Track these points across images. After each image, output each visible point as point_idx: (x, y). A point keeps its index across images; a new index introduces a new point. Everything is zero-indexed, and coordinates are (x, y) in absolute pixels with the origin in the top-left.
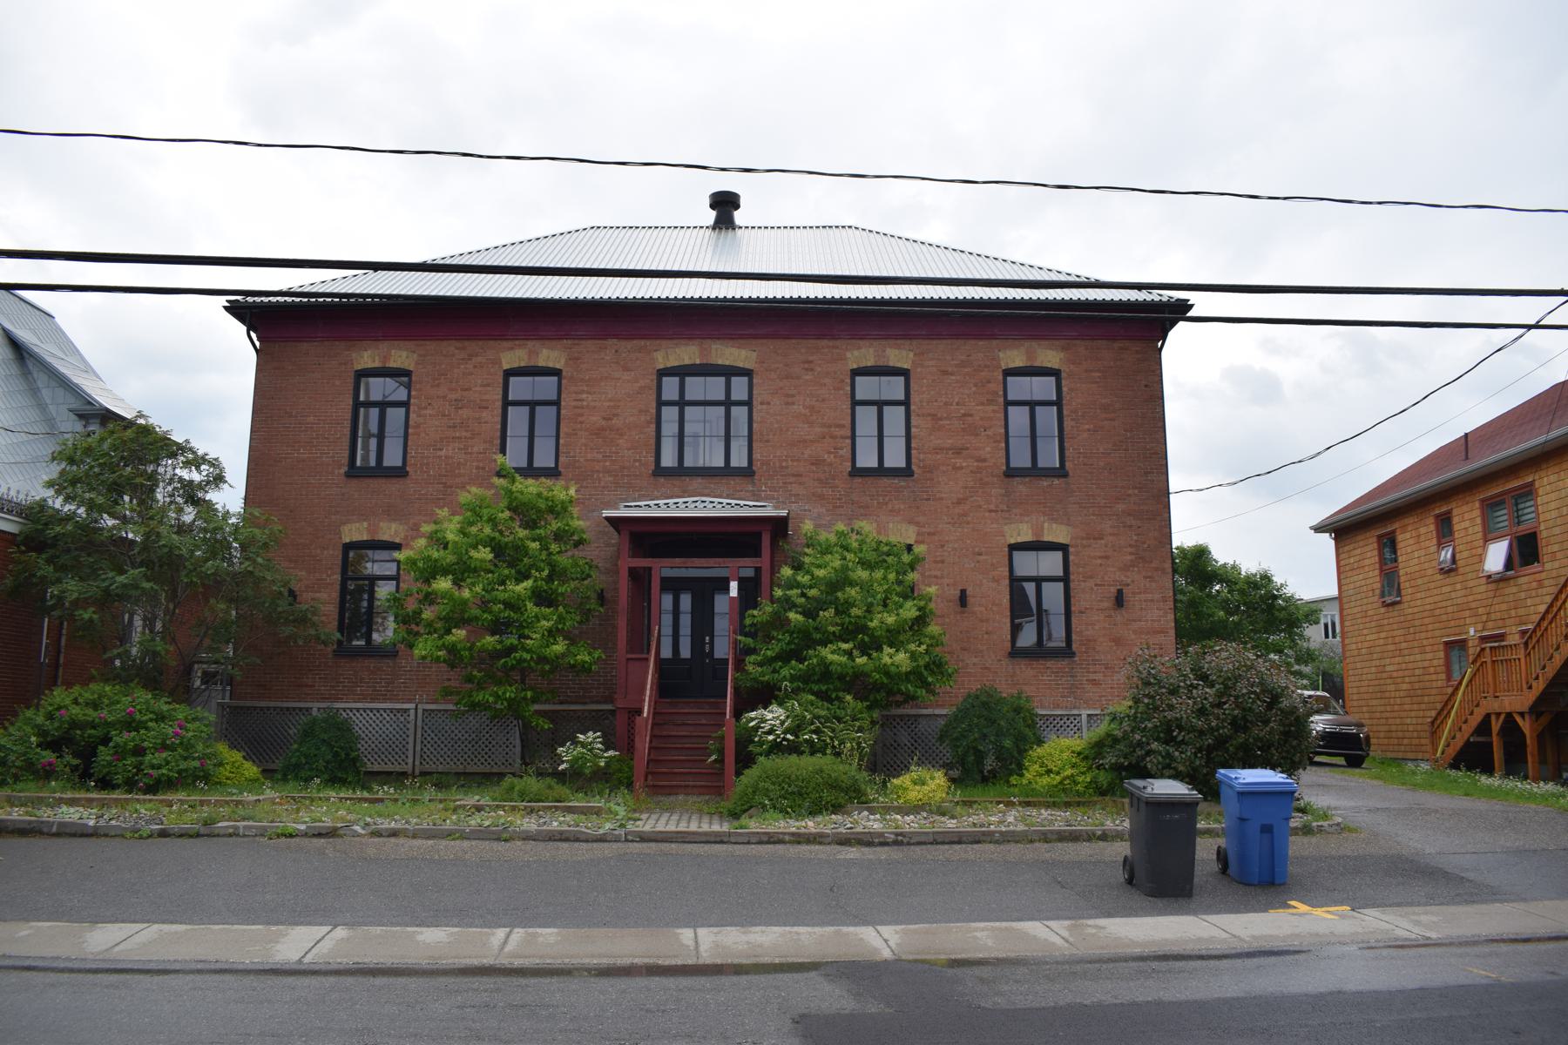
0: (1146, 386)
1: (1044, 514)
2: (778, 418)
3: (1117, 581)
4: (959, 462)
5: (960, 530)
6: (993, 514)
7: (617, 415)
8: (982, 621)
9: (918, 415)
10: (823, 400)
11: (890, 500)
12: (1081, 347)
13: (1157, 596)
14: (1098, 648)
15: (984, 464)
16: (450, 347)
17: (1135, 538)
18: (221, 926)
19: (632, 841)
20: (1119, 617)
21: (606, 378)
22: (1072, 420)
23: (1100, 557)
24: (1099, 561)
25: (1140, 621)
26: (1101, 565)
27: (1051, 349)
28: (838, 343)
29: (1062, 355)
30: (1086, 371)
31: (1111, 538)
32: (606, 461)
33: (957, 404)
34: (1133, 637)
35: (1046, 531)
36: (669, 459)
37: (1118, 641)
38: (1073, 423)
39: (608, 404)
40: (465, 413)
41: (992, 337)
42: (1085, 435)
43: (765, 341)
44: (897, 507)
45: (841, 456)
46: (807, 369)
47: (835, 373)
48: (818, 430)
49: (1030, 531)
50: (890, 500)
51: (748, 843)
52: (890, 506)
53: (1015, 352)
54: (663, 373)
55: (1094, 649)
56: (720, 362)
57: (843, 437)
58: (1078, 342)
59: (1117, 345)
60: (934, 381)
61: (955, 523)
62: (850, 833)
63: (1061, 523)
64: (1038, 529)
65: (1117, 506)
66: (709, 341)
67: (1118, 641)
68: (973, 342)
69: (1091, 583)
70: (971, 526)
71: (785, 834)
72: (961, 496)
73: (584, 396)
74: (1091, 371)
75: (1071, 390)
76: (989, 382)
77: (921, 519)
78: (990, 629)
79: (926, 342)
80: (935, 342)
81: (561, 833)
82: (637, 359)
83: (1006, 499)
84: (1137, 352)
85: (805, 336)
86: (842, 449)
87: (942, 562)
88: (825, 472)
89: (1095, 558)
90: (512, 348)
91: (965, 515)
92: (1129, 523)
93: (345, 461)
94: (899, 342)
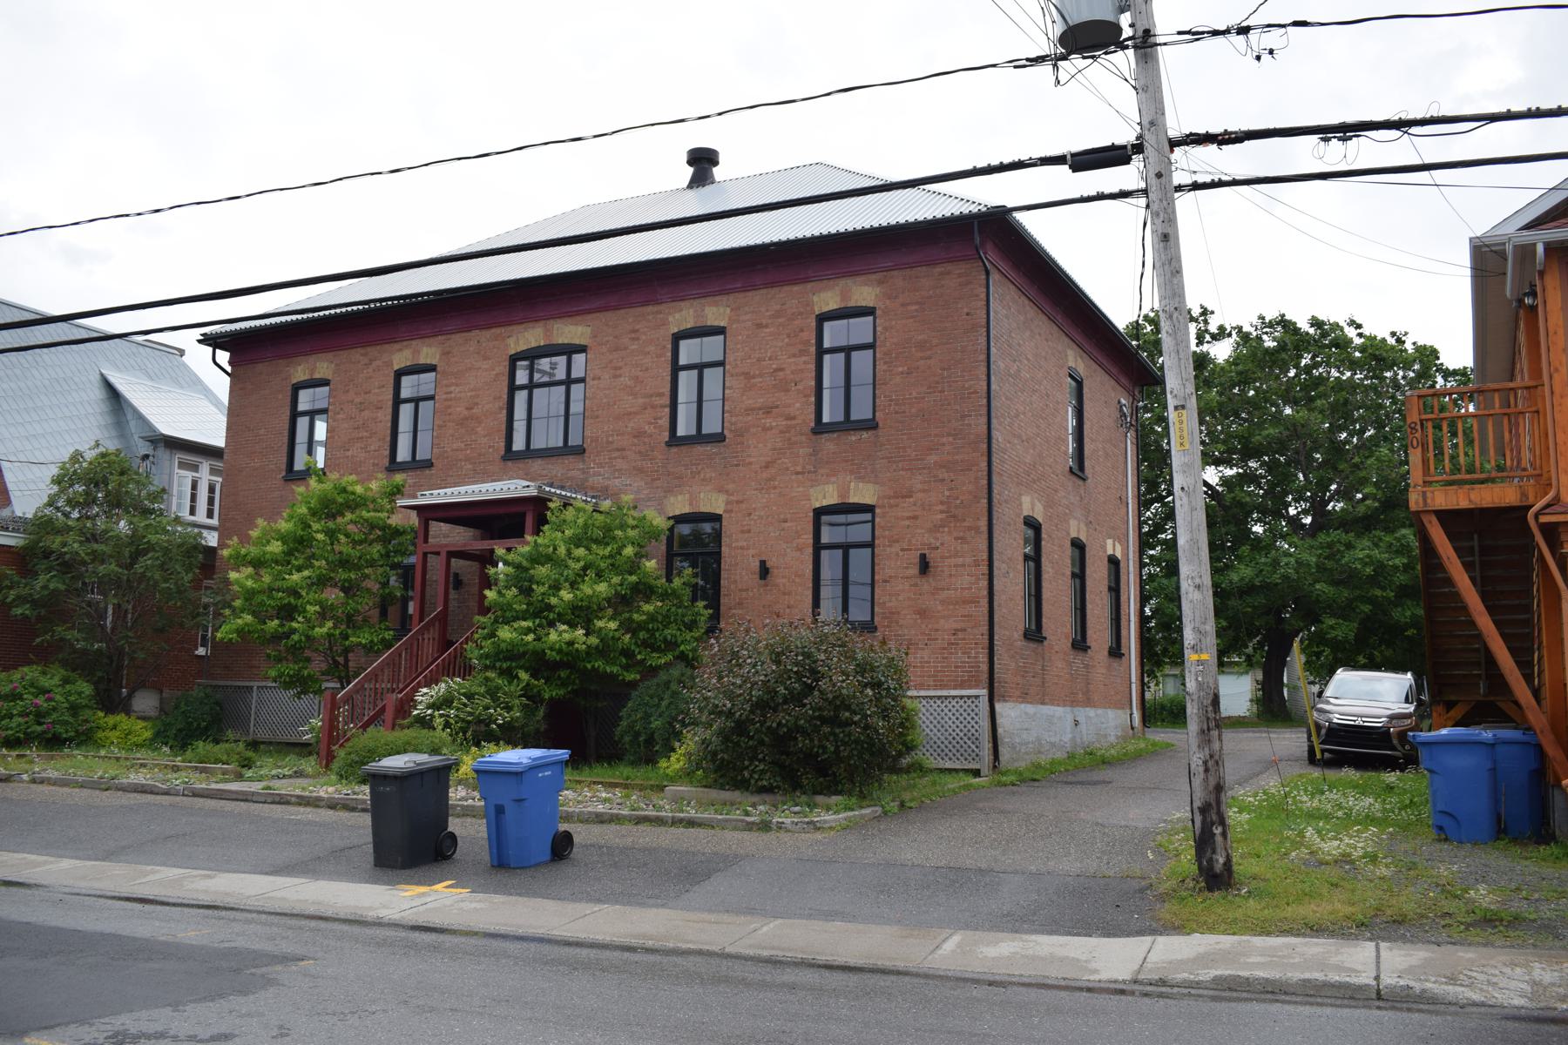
0: (968, 314)
1: (852, 472)
2: (607, 392)
3: (925, 544)
4: (768, 422)
5: (766, 496)
6: (800, 476)
7: (477, 404)
8: (784, 594)
9: (732, 376)
10: (647, 369)
11: (703, 469)
12: (898, 279)
13: (968, 560)
14: (901, 622)
15: (793, 422)
16: (356, 355)
17: (947, 493)
18: (93, 863)
19: (187, 796)
20: (926, 585)
21: (470, 369)
22: (885, 363)
23: (909, 518)
24: (907, 523)
25: (948, 589)
26: (908, 526)
27: (866, 285)
28: (662, 307)
29: (878, 290)
30: (903, 305)
31: (920, 495)
32: (466, 450)
33: (770, 359)
34: (940, 608)
35: (852, 492)
36: (519, 444)
37: (923, 613)
38: (885, 367)
39: (469, 394)
40: (366, 414)
41: (806, 280)
42: (898, 379)
43: (598, 314)
44: (708, 476)
45: (661, 426)
46: (633, 339)
47: (658, 339)
48: (641, 401)
49: (835, 493)
50: (703, 469)
51: (265, 802)
52: (702, 475)
53: (829, 294)
54: (514, 360)
55: (897, 623)
56: (560, 342)
57: (663, 406)
58: (895, 273)
59: (938, 269)
60: (748, 336)
61: (763, 489)
62: (347, 799)
63: (869, 482)
64: (844, 491)
65: (928, 458)
66: (552, 321)
67: (923, 613)
68: (787, 288)
69: (896, 548)
70: (777, 491)
71: (291, 796)
72: (769, 459)
73: (452, 388)
74: (908, 304)
75: (886, 329)
76: (802, 331)
77: (731, 487)
78: (792, 602)
79: (741, 295)
80: (750, 294)
81: (143, 785)
82: (494, 347)
83: (813, 458)
84: (960, 275)
85: (631, 305)
86: (660, 418)
87: (749, 531)
88: (645, 443)
89: (903, 519)
90: (401, 350)
91: (772, 479)
92: (941, 477)
93: (284, 467)
94: (717, 298)
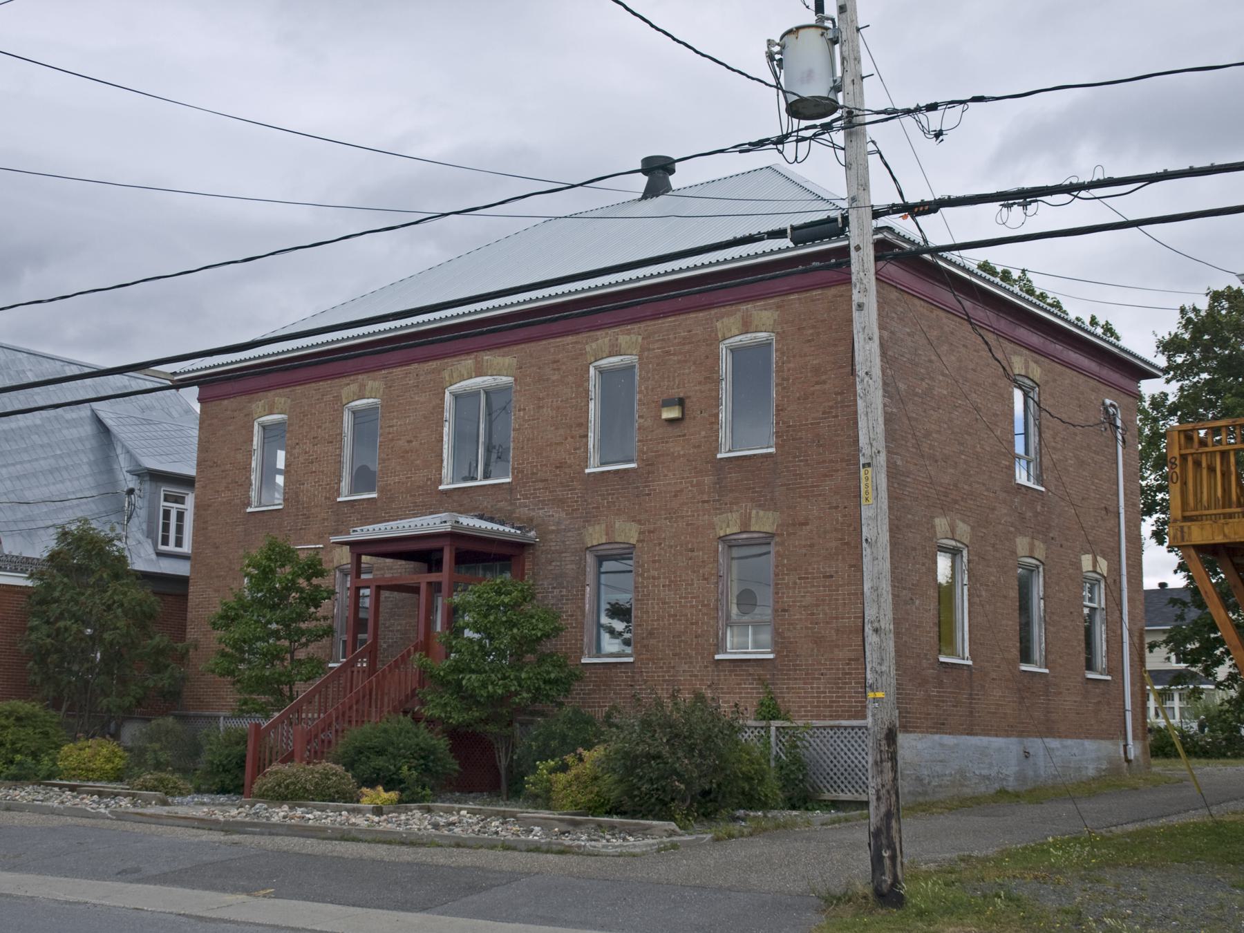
5: (675, 525)
29: (776, 314)
35: (753, 521)
49: (738, 521)
50: (618, 498)
63: (769, 510)
83: (718, 486)
90: (349, 384)
